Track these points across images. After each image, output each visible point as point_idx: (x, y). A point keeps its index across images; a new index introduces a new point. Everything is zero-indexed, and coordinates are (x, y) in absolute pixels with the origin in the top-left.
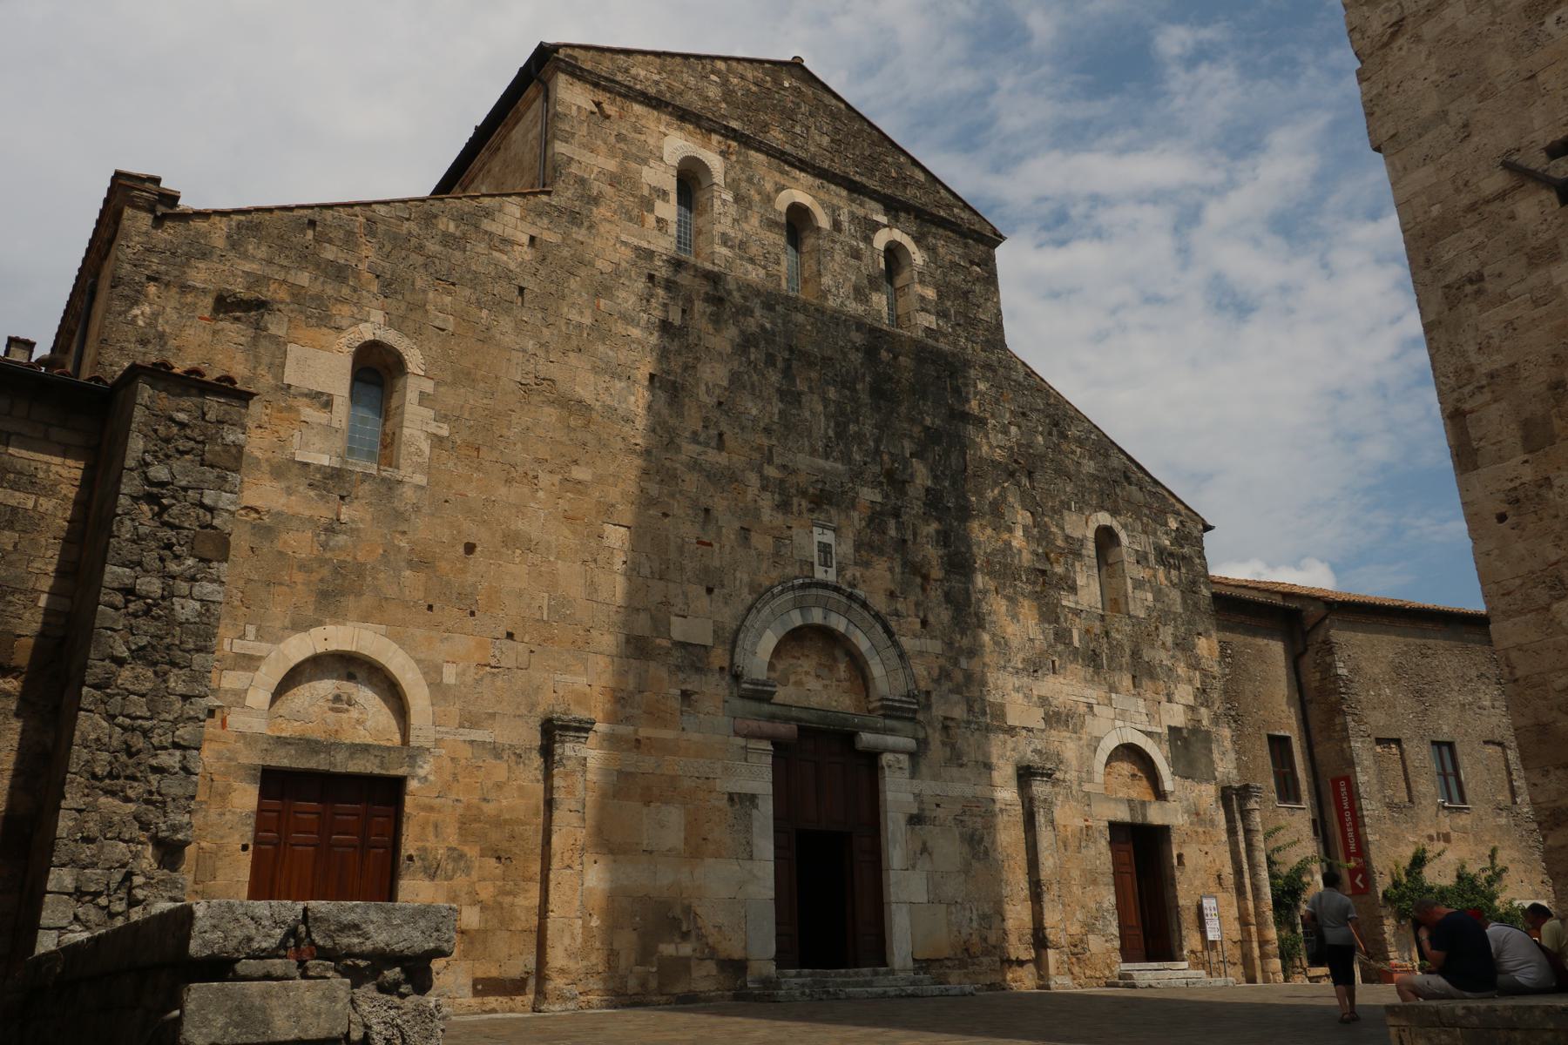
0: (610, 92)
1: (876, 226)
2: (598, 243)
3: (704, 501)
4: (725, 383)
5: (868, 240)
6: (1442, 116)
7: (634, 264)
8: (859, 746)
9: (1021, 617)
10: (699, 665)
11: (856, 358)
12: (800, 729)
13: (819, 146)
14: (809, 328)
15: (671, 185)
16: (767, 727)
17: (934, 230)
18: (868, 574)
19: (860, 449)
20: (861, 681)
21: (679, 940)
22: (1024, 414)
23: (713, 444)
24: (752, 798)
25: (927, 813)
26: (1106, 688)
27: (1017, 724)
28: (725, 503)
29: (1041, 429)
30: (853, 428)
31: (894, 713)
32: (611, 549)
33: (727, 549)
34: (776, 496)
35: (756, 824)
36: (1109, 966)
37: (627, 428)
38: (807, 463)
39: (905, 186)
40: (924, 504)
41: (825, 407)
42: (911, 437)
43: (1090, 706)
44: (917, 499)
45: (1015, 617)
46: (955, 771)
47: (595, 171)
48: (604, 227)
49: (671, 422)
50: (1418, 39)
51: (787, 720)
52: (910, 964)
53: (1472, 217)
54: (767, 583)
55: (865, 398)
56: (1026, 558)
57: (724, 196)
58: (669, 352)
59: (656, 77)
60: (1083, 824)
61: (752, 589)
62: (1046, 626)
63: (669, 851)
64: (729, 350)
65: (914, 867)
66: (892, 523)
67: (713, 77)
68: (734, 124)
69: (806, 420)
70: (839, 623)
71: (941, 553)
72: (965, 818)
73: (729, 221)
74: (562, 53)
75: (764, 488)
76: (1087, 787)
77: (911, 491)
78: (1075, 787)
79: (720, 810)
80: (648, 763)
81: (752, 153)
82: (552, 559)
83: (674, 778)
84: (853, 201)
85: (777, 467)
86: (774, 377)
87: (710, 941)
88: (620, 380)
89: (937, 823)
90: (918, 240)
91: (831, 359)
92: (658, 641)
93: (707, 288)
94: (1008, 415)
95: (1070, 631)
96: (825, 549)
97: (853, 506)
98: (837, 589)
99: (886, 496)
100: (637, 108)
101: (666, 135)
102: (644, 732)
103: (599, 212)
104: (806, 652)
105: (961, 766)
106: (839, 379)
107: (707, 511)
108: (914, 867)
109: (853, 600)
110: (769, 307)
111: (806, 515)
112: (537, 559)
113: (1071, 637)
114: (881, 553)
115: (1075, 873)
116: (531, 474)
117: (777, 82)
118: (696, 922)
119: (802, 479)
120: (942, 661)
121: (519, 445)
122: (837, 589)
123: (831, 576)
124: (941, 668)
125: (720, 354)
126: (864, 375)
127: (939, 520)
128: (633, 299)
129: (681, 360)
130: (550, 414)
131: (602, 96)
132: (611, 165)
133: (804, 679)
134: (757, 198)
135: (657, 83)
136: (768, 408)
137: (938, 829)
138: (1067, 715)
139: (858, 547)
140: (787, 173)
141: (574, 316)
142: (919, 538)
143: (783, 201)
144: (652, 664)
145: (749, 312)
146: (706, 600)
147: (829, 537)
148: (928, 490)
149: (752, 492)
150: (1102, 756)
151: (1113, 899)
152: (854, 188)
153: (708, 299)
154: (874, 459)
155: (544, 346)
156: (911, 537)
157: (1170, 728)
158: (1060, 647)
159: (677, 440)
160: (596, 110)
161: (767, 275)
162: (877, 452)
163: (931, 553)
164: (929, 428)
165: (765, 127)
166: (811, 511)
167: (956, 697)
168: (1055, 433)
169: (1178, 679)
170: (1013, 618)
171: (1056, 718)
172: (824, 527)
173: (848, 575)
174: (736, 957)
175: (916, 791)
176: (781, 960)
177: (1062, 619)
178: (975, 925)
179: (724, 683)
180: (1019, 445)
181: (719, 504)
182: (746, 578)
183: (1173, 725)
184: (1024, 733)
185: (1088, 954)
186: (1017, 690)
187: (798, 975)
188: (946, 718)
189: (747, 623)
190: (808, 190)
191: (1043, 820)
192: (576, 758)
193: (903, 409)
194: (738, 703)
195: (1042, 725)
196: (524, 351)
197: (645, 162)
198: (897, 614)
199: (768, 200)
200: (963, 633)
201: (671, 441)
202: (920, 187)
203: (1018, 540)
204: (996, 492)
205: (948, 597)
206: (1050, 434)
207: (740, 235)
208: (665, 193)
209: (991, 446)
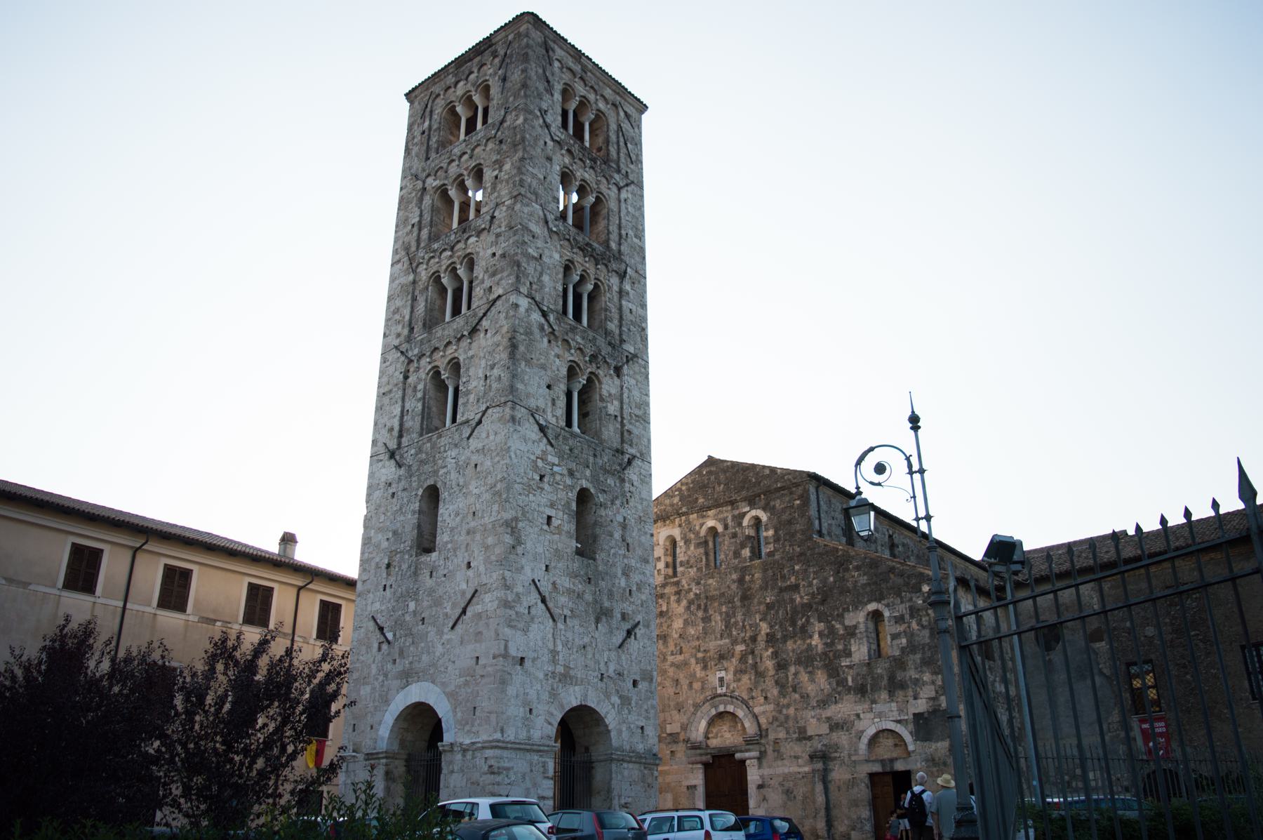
5: (740, 524)
11: (734, 587)
16: (698, 759)
18: (739, 684)
24: (695, 786)
26: (869, 703)
27: (813, 734)
30: (733, 620)
31: (749, 742)
35: (697, 796)
38: (713, 645)
43: (858, 716)
45: (812, 680)
46: (780, 763)
49: (664, 651)
51: (707, 754)
55: (738, 604)
60: (851, 777)
61: (694, 705)
66: (750, 657)
67: (677, 493)
68: (684, 509)
70: (730, 708)
71: (774, 662)
75: (697, 663)
77: (759, 638)
78: (846, 759)
83: (669, 783)
86: (700, 614)
94: (812, 575)
96: (721, 679)
98: (725, 695)
108: (759, 806)
109: (732, 697)
110: (698, 583)
113: (847, 681)
119: (711, 654)
120: (774, 713)
124: (773, 717)
127: (773, 647)
134: (692, 536)
137: (770, 790)
139: (735, 675)
143: (703, 532)
145: (690, 590)
146: (678, 716)
149: (693, 666)
150: (865, 740)
151: (868, 813)
157: (915, 715)
162: (744, 626)
163: (769, 664)
166: (716, 665)
167: (780, 729)
169: (924, 683)
171: (835, 726)
181: (681, 676)
182: (691, 702)
183: (917, 712)
184: (817, 738)
186: (813, 717)
193: (756, 600)
194: (689, 752)
198: (753, 698)
199: (698, 533)
200: (784, 697)
203: (816, 640)
204: (804, 620)
205: (777, 683)
207: (687, 558)
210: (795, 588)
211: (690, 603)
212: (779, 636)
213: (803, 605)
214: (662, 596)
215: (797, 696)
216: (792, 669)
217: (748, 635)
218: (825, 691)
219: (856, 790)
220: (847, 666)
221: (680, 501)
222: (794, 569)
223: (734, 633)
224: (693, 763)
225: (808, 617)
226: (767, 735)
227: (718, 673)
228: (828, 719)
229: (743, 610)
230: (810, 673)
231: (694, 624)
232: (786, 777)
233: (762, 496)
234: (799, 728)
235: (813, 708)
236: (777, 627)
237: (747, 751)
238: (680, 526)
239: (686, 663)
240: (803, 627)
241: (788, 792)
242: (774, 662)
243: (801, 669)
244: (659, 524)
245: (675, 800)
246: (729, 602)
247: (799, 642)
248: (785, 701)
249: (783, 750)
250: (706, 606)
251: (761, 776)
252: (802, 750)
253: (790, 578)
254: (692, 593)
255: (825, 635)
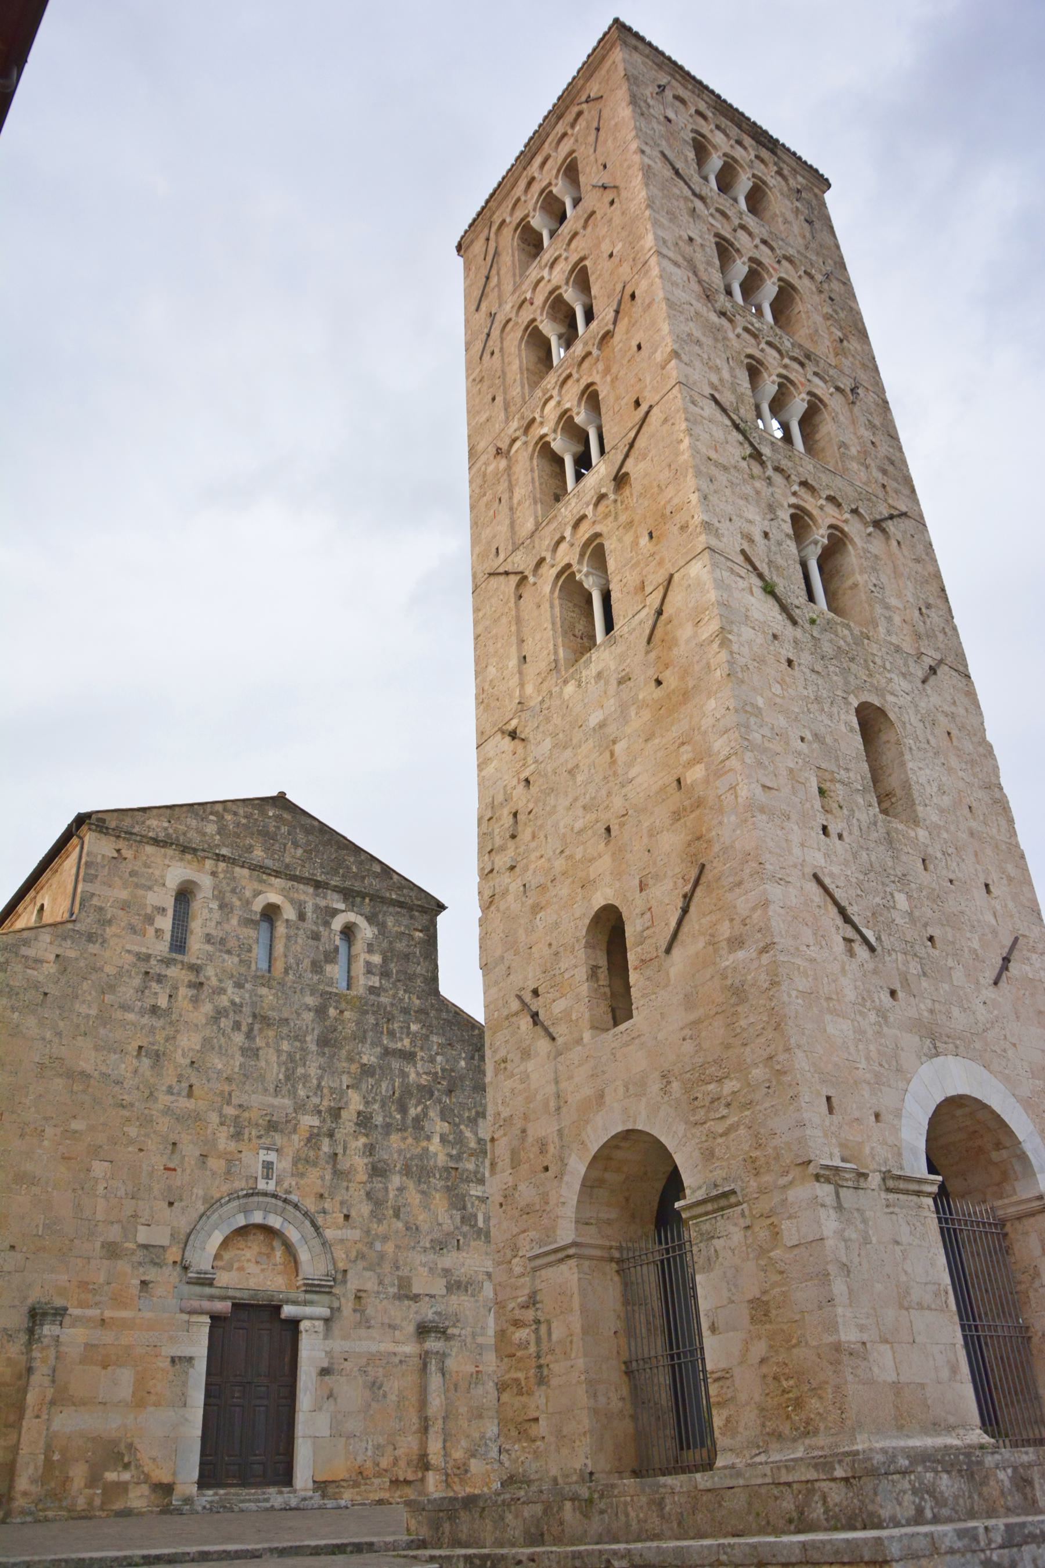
0: (128, 840)
1: (335, 912)
2: (108, 954)
3: (172, 1137)
4: (198, 1047)
5: (327, 924)
6: (502, 958)
7: (134, 965)
8: (283, 1316)
9: (432, 1207)
10: (157, 1261)
11: (309, 1016)
12: (234, 1305)
13: (293, 857)
14: (271, 998)
15: (169, 903)
16: (206, 1305)
17: (385, 908)
18: (302, 1182)
19: (304, 1086)
20: (293, 1264)
21: (120, 1469)
22: (450, 1044)
23: (184, 1093)
24: (190, 1360)
25: (336, 1366)
27: (421, 1292)
28: (190, 1137)
29: (463, 1055)
30: (300, 1071)
32: (96, 1180)
33: (188, 1171)
34: (232, 1129)
36: (487, 1484)
37: (117, 1089)
39: (363, 878)
40: (357, 1124)
41: (278, 1057)
42: (349, 1073)
44: (350, 1121)
45: (426, 1207)
46: (363, 1332)
47: (111, 900)
48: (113, 942)
49: (152, 1081)
50: (498, 910)
52: (310, 1485)
53: (506, 1023)
54: (217, 1196)
55: (313, 1047)
56: (441, 1160)
57: (211, 906)
58: (155, 1028)
59: (166, 824)
60: (473, 1369)
61: (205, 1200)
62: (454, 1212)
63: (120, 1402)
64: (204, 1021)
65: (320, 1409)
67: (212, 817)
68: (224, 851)
69: (262, 1068)
70: (275, 1221)
71: (366, 1161)
72: (369, 1369)
73: (213, 924)
74: (94, 817)
76: (480, 1340)
77: (344, 1114)
78: (469, 1340)
79: (163, 1370)
80: (107, 1337)
81: (237, 869)
82: (50, 1190)
84: (317, 895)
85: (234, 1107)
86: (239, 1038)
87: (146, 1469)
88: (115, 1053)
89: (344, 1373)
90: (371, 919)
91: (287, 1020)
92: (126, 1245)
93: (192, 977)
94: (435, 1047)
95: (475, 1216)
96: (268, 1166)
97: (295, 1130)
98: (275, 1196)
99: (324, 1121)
100: (149, 849)
101: (169, 866)
102: (108, 1314)
103: (109, 931)
104: (249, 1244)
105: (369, 1328)
106: (292, 1034)
107: (174, 1144)
108: (320, 1409)
110: (239, 985)
111: (254, 1141)
112: (35, 1190)
113: (476, 1220)
114: (315, 1164)
115: (463, 1410)
116: (39, 1129)
117: (263, 813)
118: (135, 1455)
119: (254, 1114)
121: (33, 1109)
122: (275, 1196)
123: (271, 1186)
125: (197, 1026)
126: (313, 1029)
127: (367, 1135)
128: (132, 991)
129: (164, 1034)
130: (59, 1083)
131: (121, 844)
132: (124, 895)
133: (246, 1265)
134: (238, 903)
135: (166, 829)
136: (232, 1062)
137: (343, 1379)
138: (468, 1283)
139: (295, 1162)
140: (264, 882)
141: (83, 1009)
142: (348, 1152)
143: (258, 905)
144: (120, 1263)
145: (222, 991)
146: (168, 1211)
147: (272, 1157)
148: (359, 1113)
152: (318, 885)
153: (191, 985)
154: (315, 1094)
155: (59, 1034)
156: (342, 1151)
158: (465, 1228)
159: (156, 1094)
160: (116, 855)
161: (241, 961)
163: (358, 1163)
164: (365, 1065)
165: (250, 849)
166: (260, 1137)
167: (368, 1274)
168: (477, 1057)
170: (425, 1207)
171: (455, 1286)
172: (268, 1149)
173: (286, 1185)
174: (165, 1481)
175: (328, 1349)
176: (203, 1483)
177: (469, 1206)
178: (369, 1453)
179: (175, 1273)
180: (443, 1070)
182: (201, 1193)
184: (427, 1299)
185: (469, 1475)
187: (216, 1494)
188: (359, 1291)
189: (198, 1227)
190: (283, 892)
191: (433, 1369)
192: (51, 1336)
194: (186, 1289)
195: (444, 1291)
196: (43, 1039)
197: (150, 888)
199: (248, 903)
200: (380, 1221)
201: (151, 1094)
202: (376, 876)
203: (435, 1146)
204: (419, 1109)
206: (473, 1058)
207: (221, 934)
208: (164, 910)
209: (418, 1074)
210: (409, 1056)
211: (219, 1014)
212: (378, 1120)
213: (420, 1088)
214: (160, 979)
215: (400, 1225)
216: (396, 1180)
217: (326, 1103)
218: (445, 1227)
219: (480, 1390)
220: (478, 1197)
221: (219, 833)
222: (409, 1028)
223: (302, 1093)
224: (191, 1313)
225: (426, 1107)
226: (344, 1281)
227: (262, 1152)
228: (447, 1272)
229: (321, 1060)
230: (423, 1193)
231: (222, 1052)
232: (372, 1359)
233: (367, 900)
234: (400, 1278)
235: (425, 1250)
236: (376, 1106)
237: (306, 1303)
238: (214, 874)
239: (197, 1117)
240: (417, 1120)
241: (374, 1386)
242: (366, 1161)
243: (411, 1185)
244: (170, 852)
245: (140, 1383)
246: (296, 1038)
247: (410, 1140)
248: (382, 1229)
249: (370, 1311)
250: (251, 1030)
251: (327, 1352)
252: (406, 1317)
253: (401, 1040)
254: (224, 998)
255: (449, 1142)
